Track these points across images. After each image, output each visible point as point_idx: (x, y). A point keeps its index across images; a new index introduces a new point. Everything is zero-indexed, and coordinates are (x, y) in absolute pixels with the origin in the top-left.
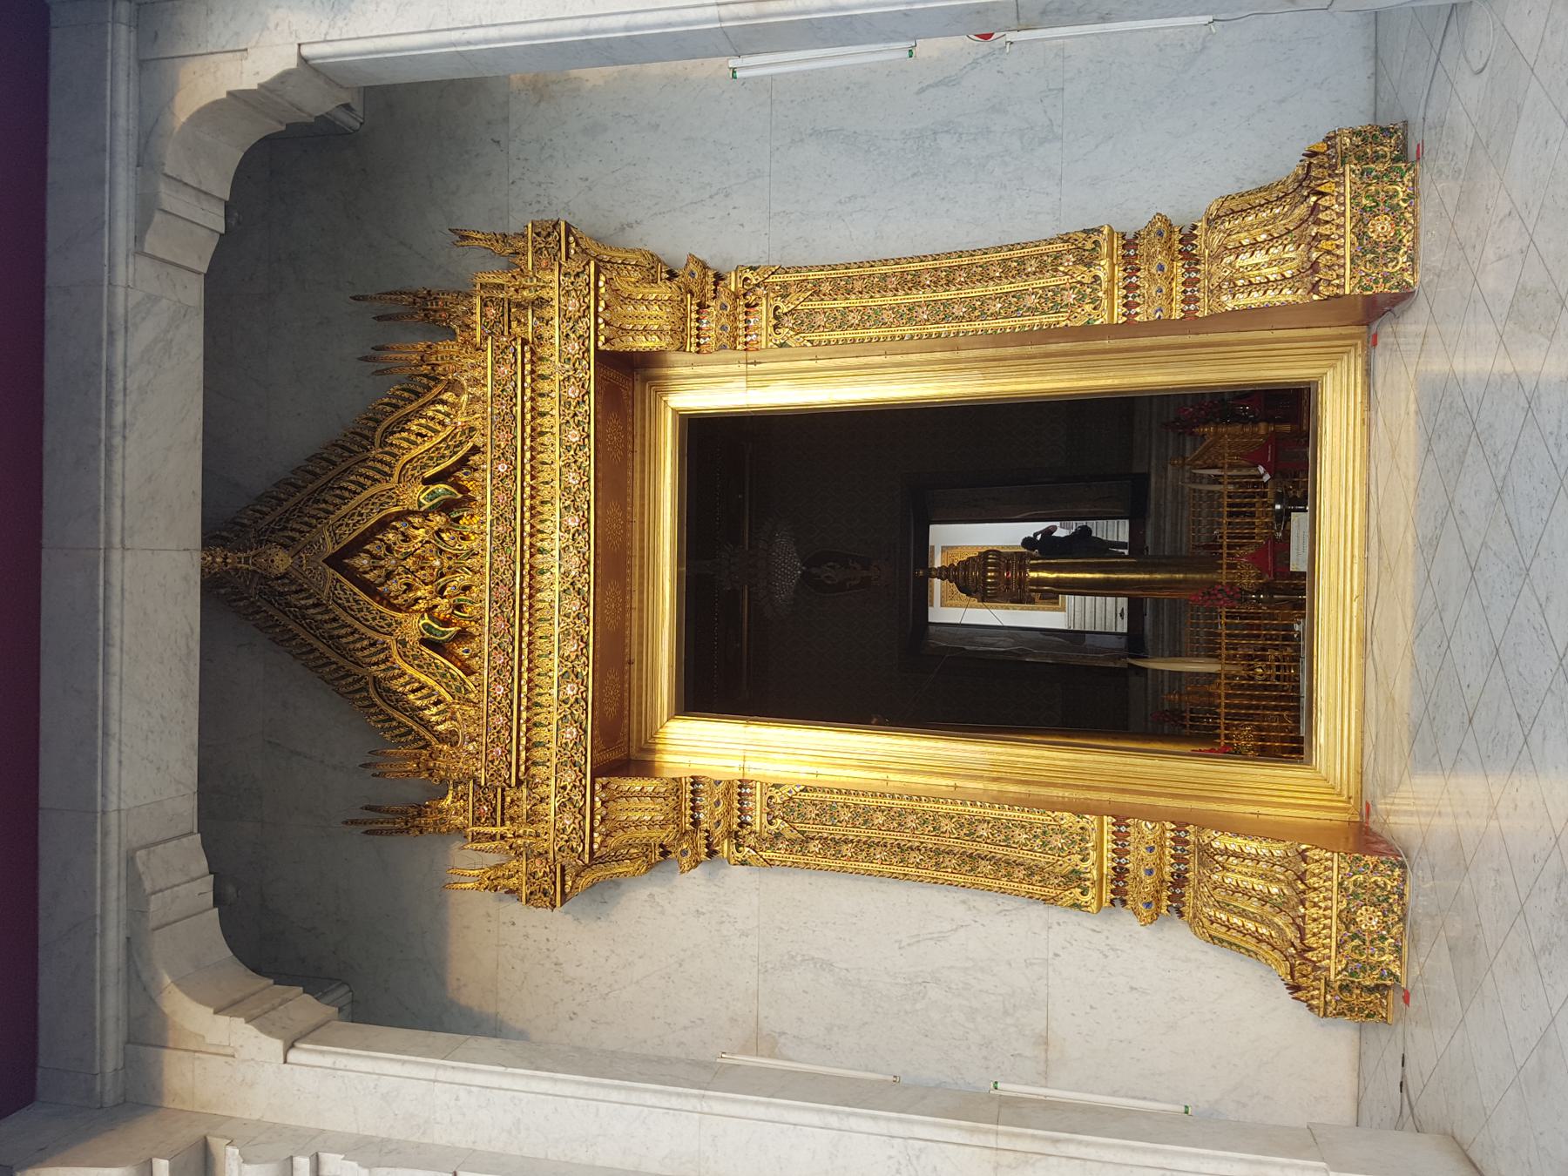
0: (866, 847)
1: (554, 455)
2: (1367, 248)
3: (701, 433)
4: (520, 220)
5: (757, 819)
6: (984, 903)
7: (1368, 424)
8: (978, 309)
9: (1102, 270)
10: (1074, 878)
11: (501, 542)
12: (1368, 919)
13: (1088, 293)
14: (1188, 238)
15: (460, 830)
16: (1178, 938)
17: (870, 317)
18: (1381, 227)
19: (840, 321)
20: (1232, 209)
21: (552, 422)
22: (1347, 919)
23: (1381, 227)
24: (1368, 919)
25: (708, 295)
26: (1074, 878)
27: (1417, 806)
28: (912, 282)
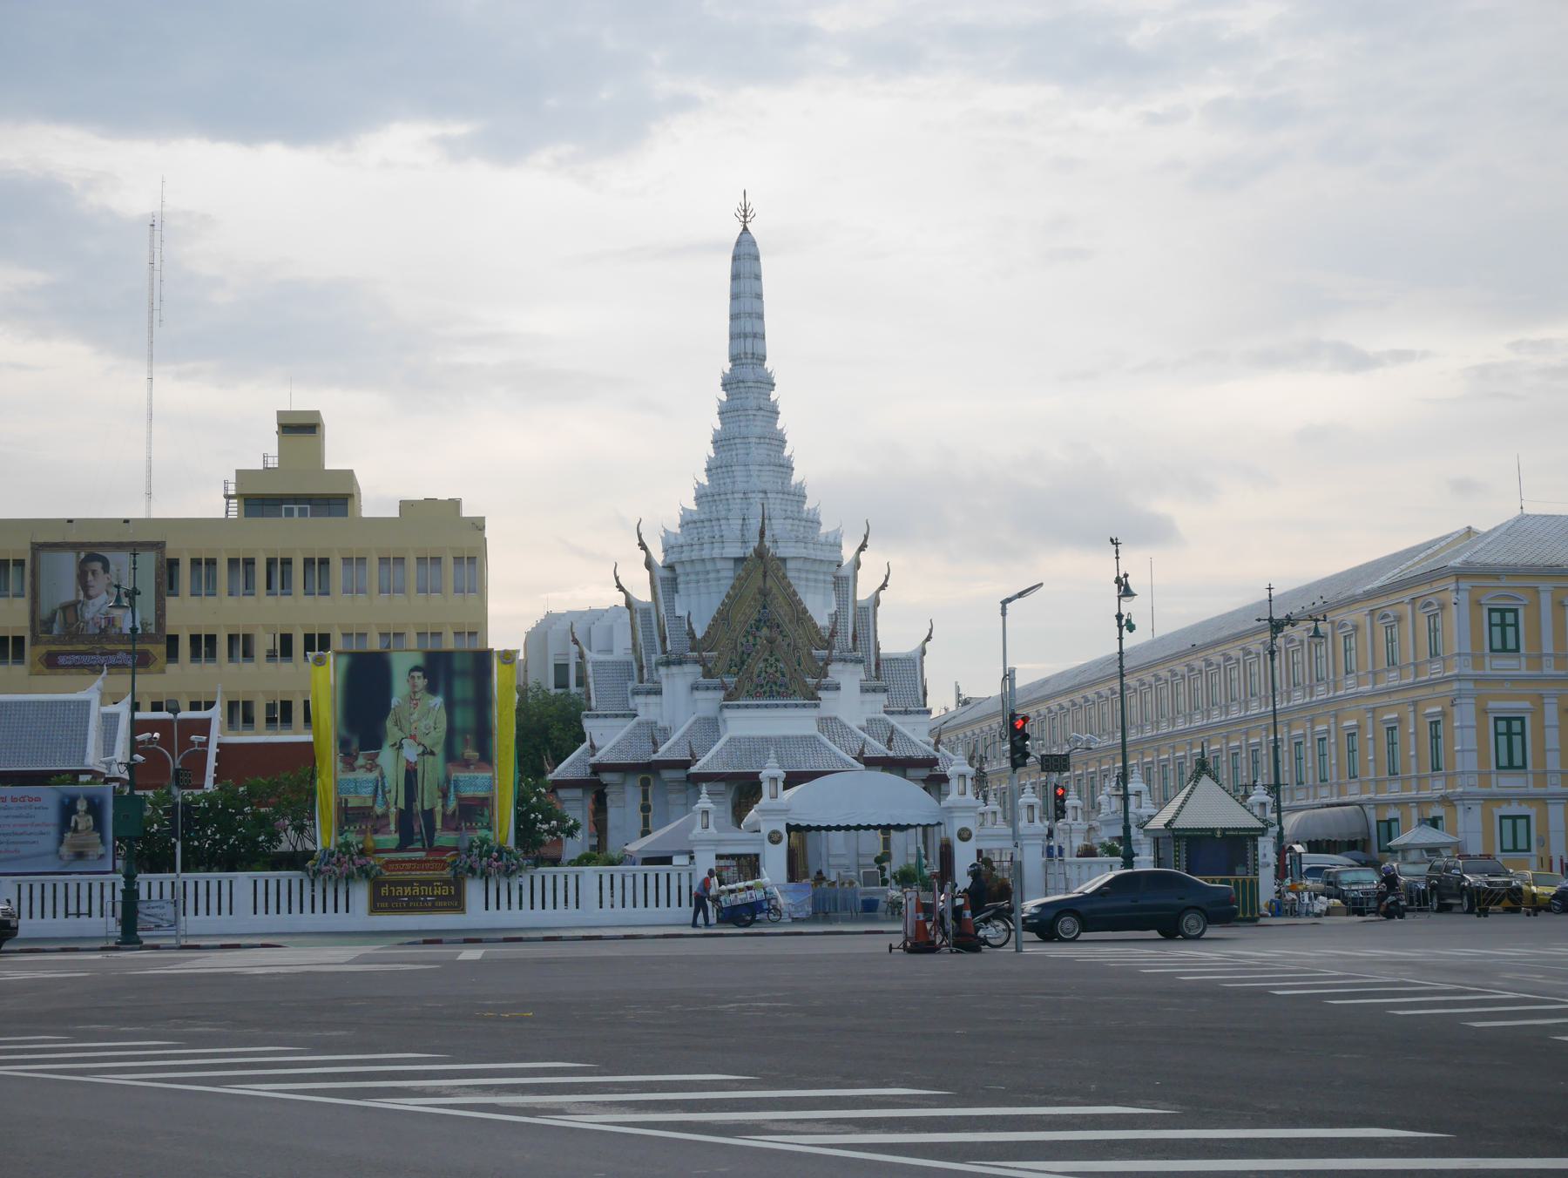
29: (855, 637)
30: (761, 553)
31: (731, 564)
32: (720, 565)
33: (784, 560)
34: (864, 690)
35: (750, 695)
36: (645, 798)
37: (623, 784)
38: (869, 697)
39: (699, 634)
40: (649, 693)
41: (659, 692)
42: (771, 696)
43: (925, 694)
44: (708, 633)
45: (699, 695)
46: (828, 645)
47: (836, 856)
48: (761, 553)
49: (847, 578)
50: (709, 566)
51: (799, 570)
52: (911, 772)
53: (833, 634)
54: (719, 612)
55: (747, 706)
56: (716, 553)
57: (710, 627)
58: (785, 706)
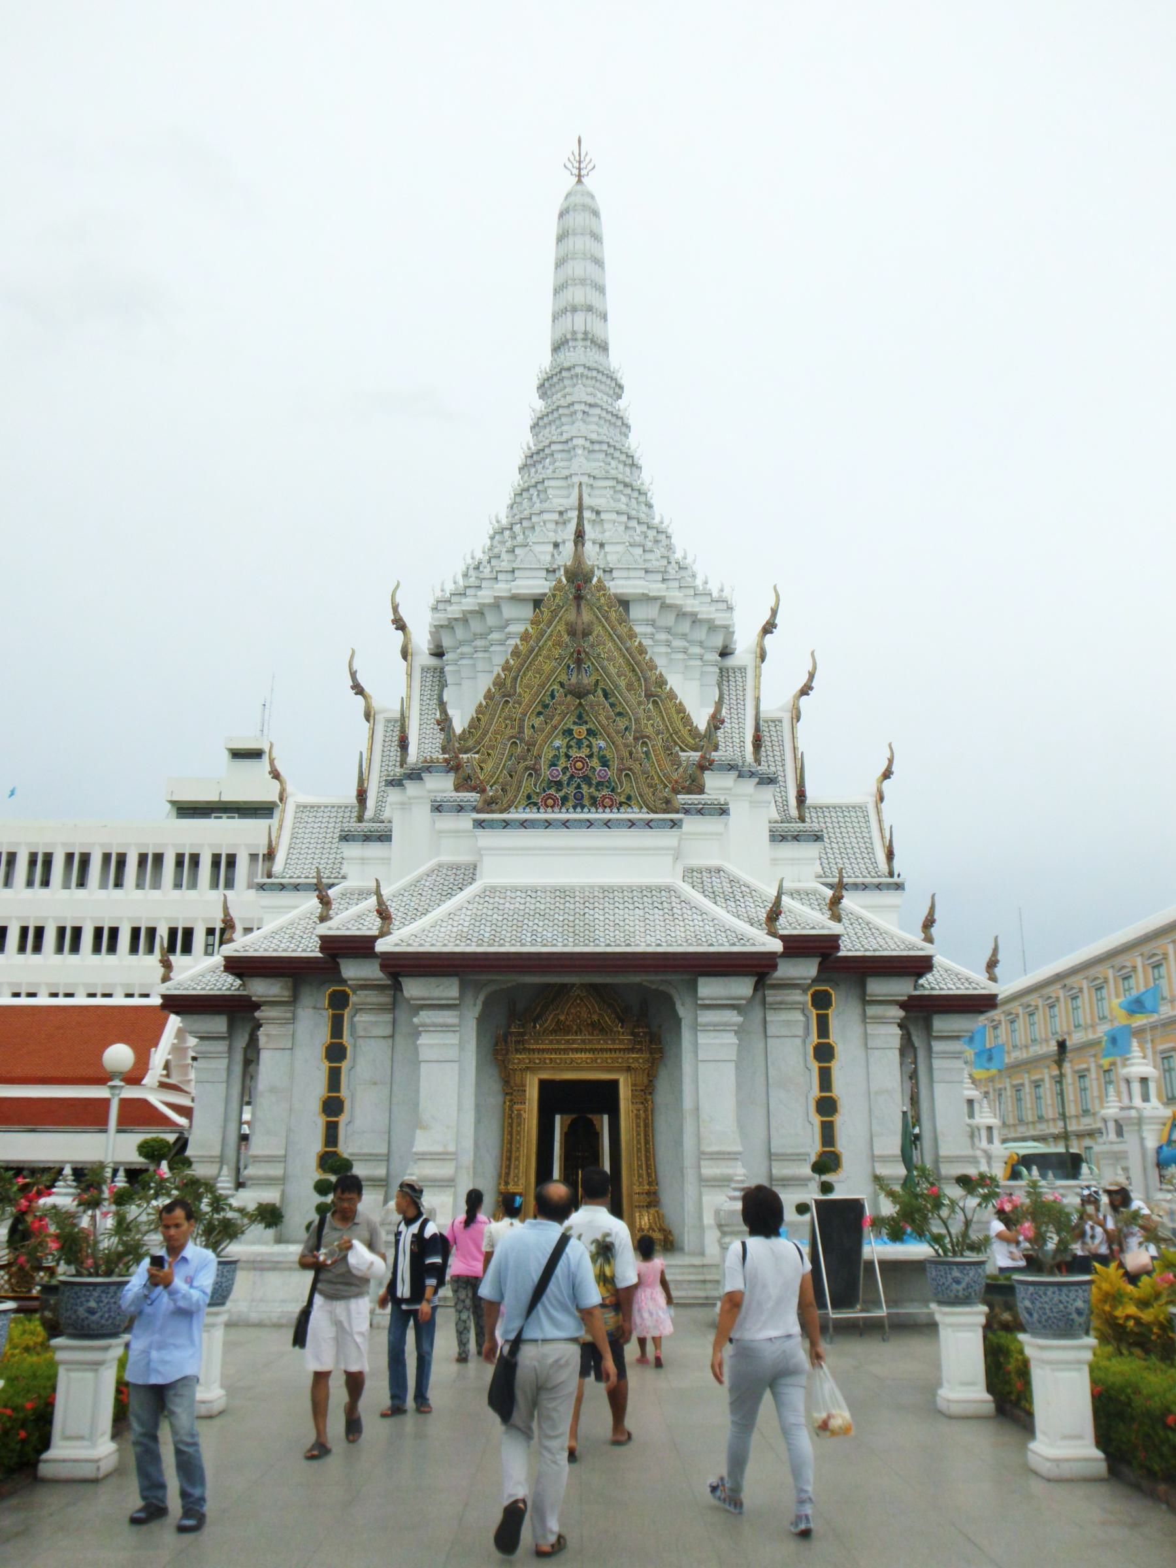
0: (511, 1134)
1: (605, 1055)
3: (614, 1084)
5: (516, 1107)
8: (639, 1159)
9: (647, 1187)
10: (507, 1183)
11: (583, 1041)
13: (641, 1184)
17: (638, 1134)
19: (638, 1126)
25: (646, 1092)
28: (647, 1142)
29: (757, 743)
30: (578, 580)
31: (528, 612)
32: (508, 611)
33: (624, 603)
34: (779, 837)
35: (530, 802)
37: (294, 1001)
38: (789, 850)
40: (367, 838)
41: (384, 837)
42: (579, 805)
43: (890, 855)
44: (475, 723)
45: (448, 822)
46: (708, 739)
48: (578, 580)
49: (742, 670)
50: (491, 619)
51: (652, 623)
52: (877, 987)
53: (716, 722)
54: (499, 683)
55: (523, 824)
56: (502, 588)
57: (480, 710)
58: (607, 824)
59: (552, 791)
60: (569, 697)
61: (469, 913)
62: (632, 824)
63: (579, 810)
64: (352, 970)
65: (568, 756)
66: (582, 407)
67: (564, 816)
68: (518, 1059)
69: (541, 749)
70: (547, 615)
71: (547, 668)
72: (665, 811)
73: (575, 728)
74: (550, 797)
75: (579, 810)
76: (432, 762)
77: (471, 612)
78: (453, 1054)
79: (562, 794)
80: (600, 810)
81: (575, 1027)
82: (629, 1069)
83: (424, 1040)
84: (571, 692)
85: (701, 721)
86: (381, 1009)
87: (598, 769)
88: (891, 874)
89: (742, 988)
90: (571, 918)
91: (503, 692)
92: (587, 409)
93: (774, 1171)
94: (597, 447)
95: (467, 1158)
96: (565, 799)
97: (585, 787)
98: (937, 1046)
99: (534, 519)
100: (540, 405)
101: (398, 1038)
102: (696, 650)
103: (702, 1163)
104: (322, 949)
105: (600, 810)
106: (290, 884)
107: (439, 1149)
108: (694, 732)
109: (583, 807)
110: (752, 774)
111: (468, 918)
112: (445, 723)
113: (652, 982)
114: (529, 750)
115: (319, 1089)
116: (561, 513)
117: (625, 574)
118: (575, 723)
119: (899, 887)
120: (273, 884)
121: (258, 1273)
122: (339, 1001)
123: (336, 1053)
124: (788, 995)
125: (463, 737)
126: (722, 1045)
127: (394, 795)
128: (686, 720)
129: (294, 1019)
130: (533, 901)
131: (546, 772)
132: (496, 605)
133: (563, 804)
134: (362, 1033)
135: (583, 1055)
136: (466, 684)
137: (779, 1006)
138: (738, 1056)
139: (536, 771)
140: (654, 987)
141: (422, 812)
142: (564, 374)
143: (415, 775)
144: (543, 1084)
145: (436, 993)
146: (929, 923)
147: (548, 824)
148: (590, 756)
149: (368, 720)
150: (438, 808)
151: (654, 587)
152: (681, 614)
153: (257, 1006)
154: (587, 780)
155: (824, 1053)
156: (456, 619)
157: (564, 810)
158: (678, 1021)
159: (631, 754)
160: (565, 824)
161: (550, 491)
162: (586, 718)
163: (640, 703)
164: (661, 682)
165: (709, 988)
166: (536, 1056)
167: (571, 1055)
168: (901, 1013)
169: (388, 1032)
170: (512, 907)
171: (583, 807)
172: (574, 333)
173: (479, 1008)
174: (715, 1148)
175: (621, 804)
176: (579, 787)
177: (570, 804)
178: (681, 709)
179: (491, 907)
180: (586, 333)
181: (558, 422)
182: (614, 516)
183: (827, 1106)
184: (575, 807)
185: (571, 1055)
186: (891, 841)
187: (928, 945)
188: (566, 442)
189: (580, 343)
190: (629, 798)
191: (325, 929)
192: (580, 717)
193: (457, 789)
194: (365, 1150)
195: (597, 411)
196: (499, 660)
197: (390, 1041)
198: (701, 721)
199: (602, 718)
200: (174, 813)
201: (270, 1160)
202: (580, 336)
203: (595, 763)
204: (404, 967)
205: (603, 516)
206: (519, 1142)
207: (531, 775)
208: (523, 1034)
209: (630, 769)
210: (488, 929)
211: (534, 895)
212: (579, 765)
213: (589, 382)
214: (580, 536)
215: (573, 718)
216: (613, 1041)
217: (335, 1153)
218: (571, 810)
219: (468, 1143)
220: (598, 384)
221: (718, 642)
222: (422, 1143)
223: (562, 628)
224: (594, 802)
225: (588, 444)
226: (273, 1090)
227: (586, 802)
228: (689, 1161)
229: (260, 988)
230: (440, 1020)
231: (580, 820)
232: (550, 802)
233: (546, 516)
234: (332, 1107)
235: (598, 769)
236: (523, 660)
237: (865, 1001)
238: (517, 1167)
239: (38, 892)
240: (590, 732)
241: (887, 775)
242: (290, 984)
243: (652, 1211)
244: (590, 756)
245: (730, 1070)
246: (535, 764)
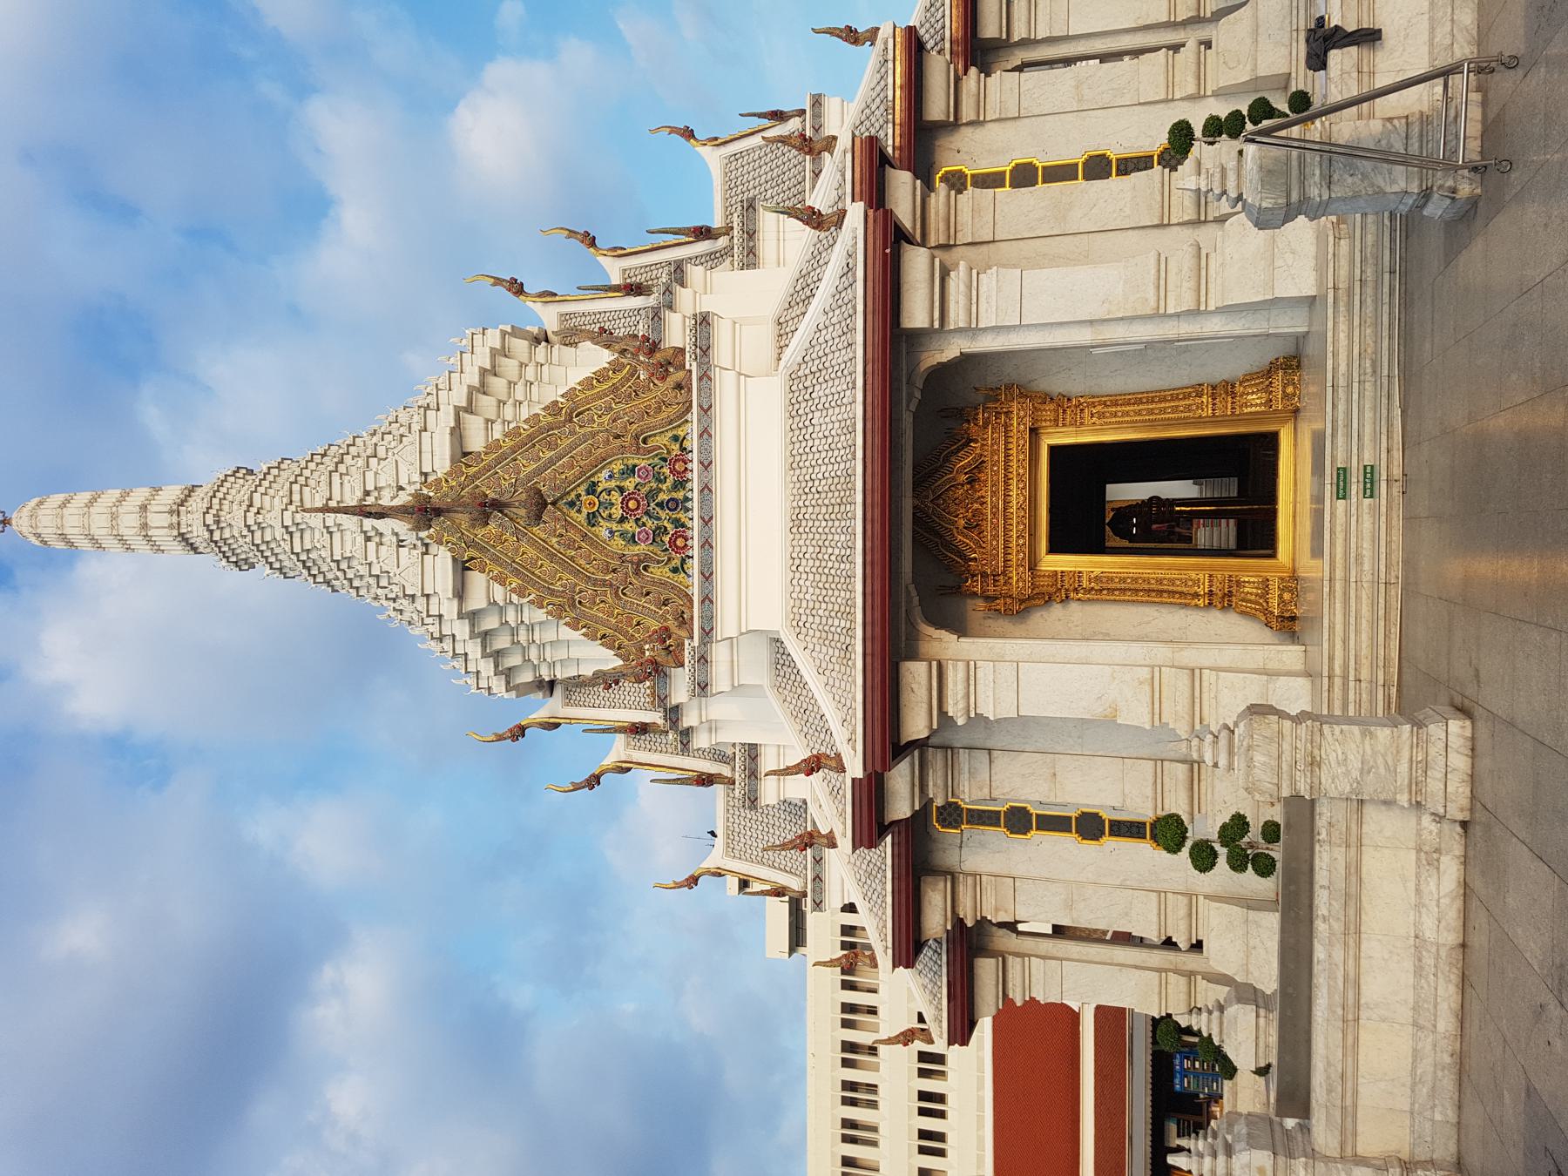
0: (1123, 590)
1: (1014, 464)
2: (1286, 396)
4: (992, 381)
6: (1164, 610)
7: (1295, 445)
8: (1163, 411)
10: (1196, 595)
11: (994, 493)
12: (1287, 596)
13: (1200, 406)
14: (1233, 386)
15: (975, 594)
16: (1232, 617)
17: (1127, 414)
18: (1290, 390)
20: (1248, 378)
21: (1014, 452)
22: (1280, 597)
23: (1290, 390)
24: (1287, 596)
26: (1196, 595)
27: (1309, 568)
30: (424, 512)
32: (476, 601)
36: (985, 818)
37: (952, 875)
39: (610, 661)
45: (720, 677)
47: (1161, 285)
48: (424, 512)
52: (936, 108)
53: (604, 337)
54: (558, 613)
55: (707, 577)
56: (450, 609)
58: (706, 466)
59: (666, 539)
60: (544, 518)
61: (817, 648)
62: (705, 433)
63: (689, 505)
64: (901, 807)
65: (622, 520)
66: (250, 515)
67: (696, 524)
68: (1018, 580)
69: (612, 555)
70: (472, 553)
71: (532, 552)
72: (690, 390)
73: (585, 511)
74: (672, 542)
75: (689, 505)
76: (653, 694)
77: (484, 647)
78: (1007, 670)
79: (669, 526)
80: (689, 475)
81: (976, 506)
82: (1034, 432)
83: (987, 710)
84: (538, 517)
85: (602, 357)
86: (951, 767)
87: (638, 480)
88: (802, 112)
89: (917, 263)
90: (824, 510)
91: (568, 608)
92: (254, 510)
93: (1186, 218)
94: (296, 497)
95: (1161, 653)
96: (678, 523)
97: (663, 497)
98: (1019, 32)
99: (375, 571)
100: (262, 569)
101: (988, 745)
102: (530, 373)
103: (1170, 311)
104: (872, 845)
105: (689, 475)
106: (813, 869)
107: (1147, 688)
108: (616, 367)
109: (687, 499)
110: (668, 290)
111: (824, 649)
112: (608, 680)
113: (910, 396)
114: (614, 571)
115: (1067, 844)
116: (368, 539)
117: (426, 457)
118: (579, 511)
119: (817, 101)
120: (814, 891)
121: (1363, 1015)
122: (953, 814)
123: (1019, 821)
124: (937, 213)
125: (625, 658)
126: (999, 289)
127: (701, 741)
128: (600, 376)
129: (974, 875)
130: (804, 562)
131: (641, 549)
132: (473, 617)
133: (683, 525)
134: (986, 791)
135: (1014, 493)
136: (575, 652)
137: (950, 223)
138: (1015, 266)
139: (640, 561)
140: (918, 395)
141: (717, 709)
142: (216, 536)
143: (673, 714)
144: (1053, 549)
145: (921, 692)
146: (851, 36)
147: (707, 544)
148: (621, 489)
149: (629, 769)
150: (702, 688)
151: (446, 419)
152: (483, 389)
153: (959, 922)
154: (652, 495)
155: (1024, 176)
156: (496, 666)
157: (689, 524)
158: (966, 360)
159: (617, 437)
160: (707, 521)
161: (307, 546)
162: (573, 495)
163: (573, 433)
164: (554, 408)
165: (917, 314)
166: (1013, 557)
167: (1014, 510)
168: (973, 71)
169: (984, 756)
170: (811, 590)
171: (687, 499)
172: (171, 526)
173: (943, 634)
174: (1151, 294)
175: (683, 449)
176: (660, 505)
177: (681, 515)
178: (587, 383)
179: (810, 619)
180: (171, 512)
181: (273, 545)
182: (370, 476)
183: (1098, 167)
184: (687, 510)
185: (1014, 510)
186: (760, 115)
187: (881, 34)
188: (291, 534)
189: (183, 518)
190: (675, 438)
191: (845, 843)
192: (572, 504)
193: (682, 665)
194: (1149, 792)
195: (257, 496)
196: (540, 615)
197: (995, 754)
198: (602, 357)
199: (570, 474)
200: (801, 950)
201: (1162, 913)
202: (175, 519)
203: (629, 484)
204: (887, 740)
205: (370, 487)
206: (1135, 580)
207: (645, 568)
208: (984, 575)
209: (637, 437)
210: (836, 622)
211: (797, 562)
212: (632, 504)
213: (226, 507)
214: (362, 511)
215: (573, 513)
216: (994, 452)
217: (1153, 826)
218: (689, 514)
219: (1137, 651)
220: (229, 497)
221: (520, 346)
222: (1136, 714)
223: (481, 532)
224: (681, 484)
225: (292, 508)
226: (1069, 906)
227: (680, 495)
228: (1169, 330)
229: (935, 921)
230: (961, 687)
231: (702, 502)
232: (680, 542)
233: (372, 557)
234: (1090, 826)
235: (638, 480)
236: (526, 580)
237: (952, 125)
238: (1172, 581)
239: (882, 1097)
240: (592, 490)
241: (688, 134)
242: (930, 879)
243: (1239, 389)
244: (621, 489)
245: (1037, 279)
246: (632, 562)
